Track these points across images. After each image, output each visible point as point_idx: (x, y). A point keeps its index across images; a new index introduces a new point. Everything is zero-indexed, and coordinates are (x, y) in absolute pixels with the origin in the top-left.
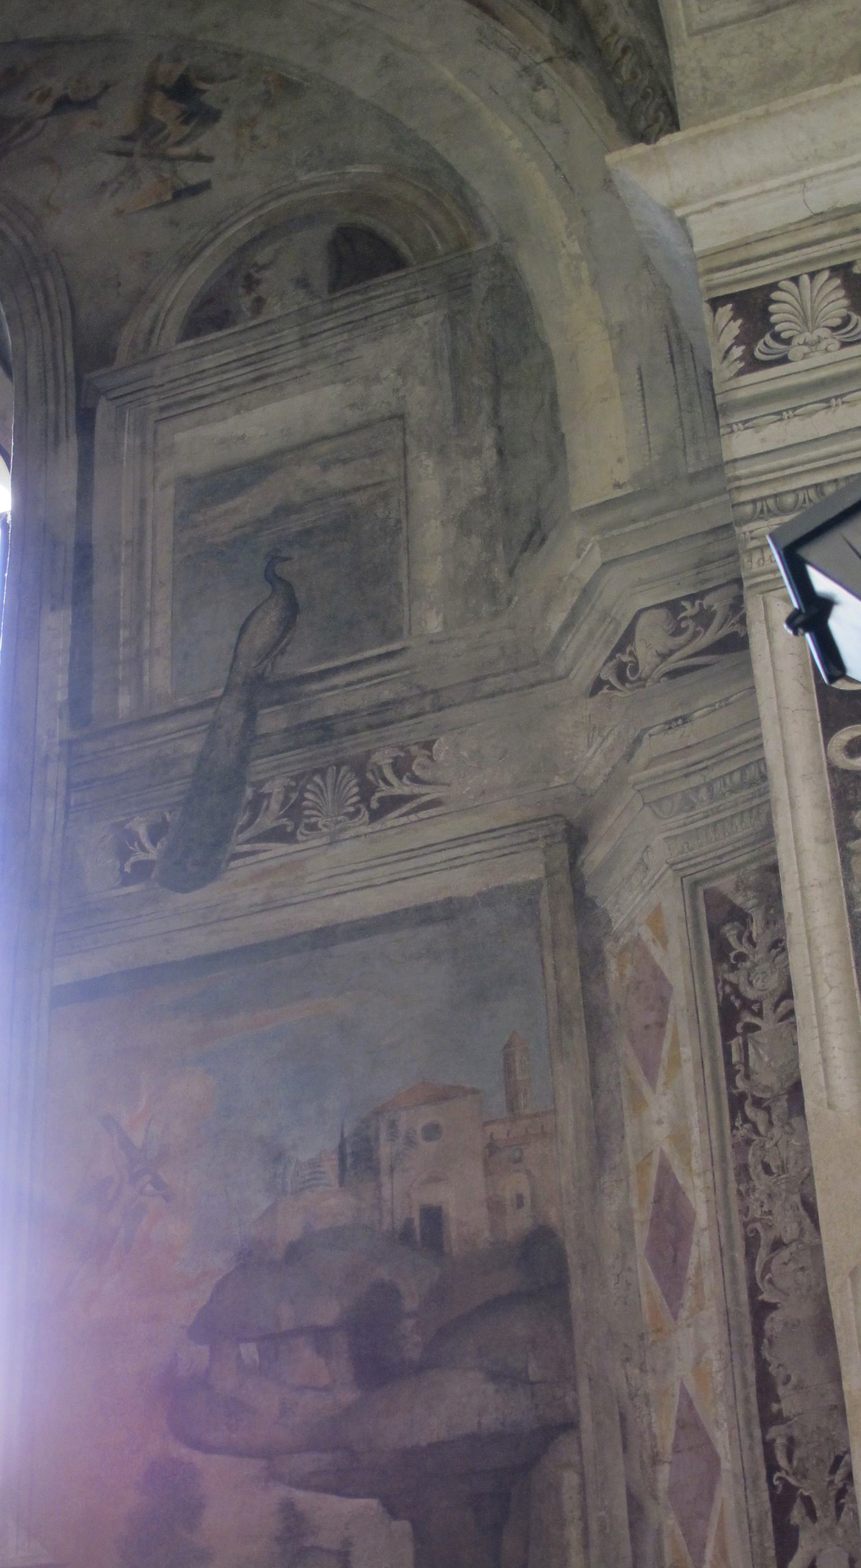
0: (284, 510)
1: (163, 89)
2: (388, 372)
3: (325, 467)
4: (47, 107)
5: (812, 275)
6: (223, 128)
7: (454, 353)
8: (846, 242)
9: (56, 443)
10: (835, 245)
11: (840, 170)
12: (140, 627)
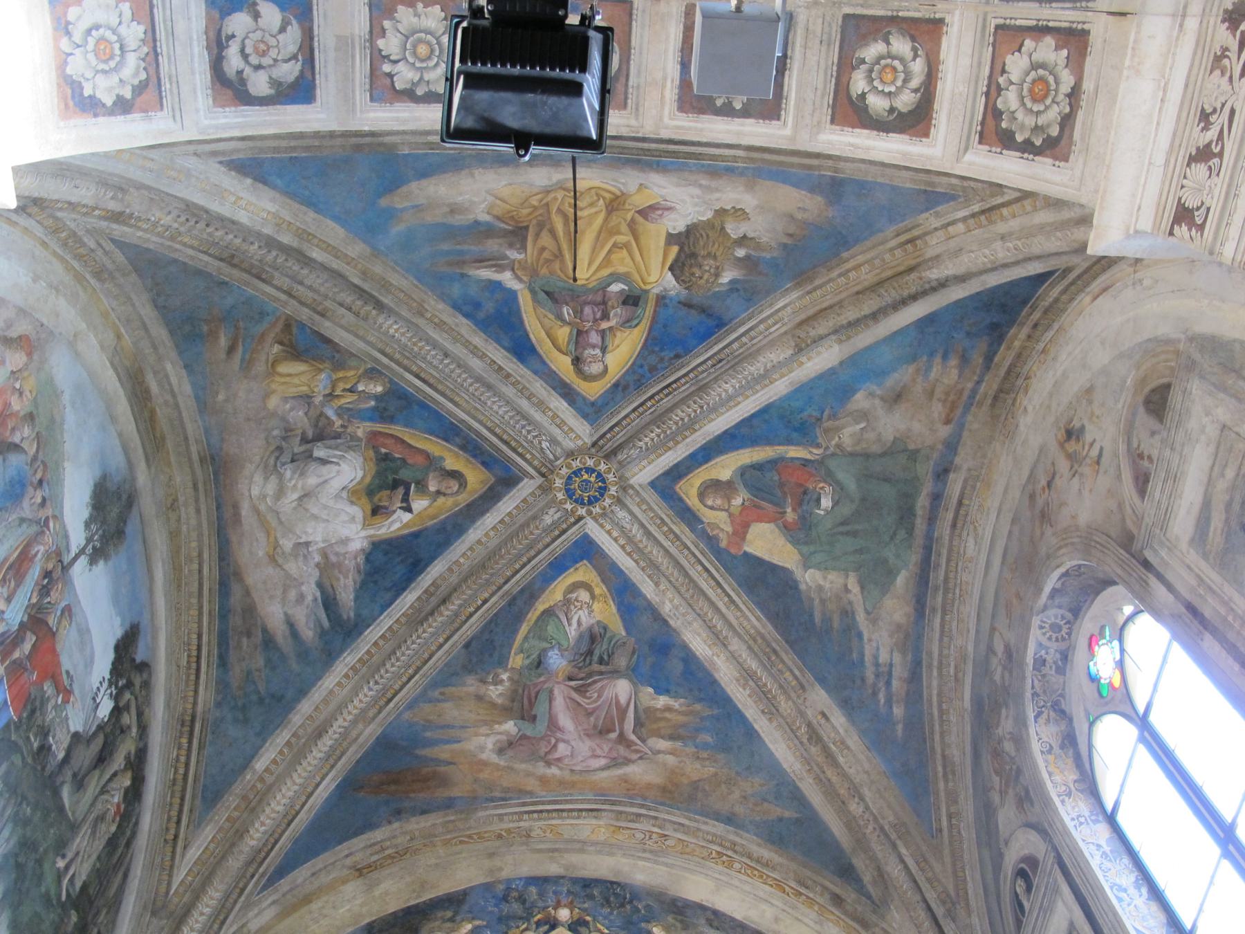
0: (1228, 506)
1: (1065, 441)
2: (1205, 420)
3: (1223, 475)
4: (1047, 491)
5: (1185, 177)
6: (1089, 427)
7: (1214, 384)
8: (1182, 153)
9: (1147, 584)
10: (1180, 159)
11: (1154, 142)
12: (1232, 610)
